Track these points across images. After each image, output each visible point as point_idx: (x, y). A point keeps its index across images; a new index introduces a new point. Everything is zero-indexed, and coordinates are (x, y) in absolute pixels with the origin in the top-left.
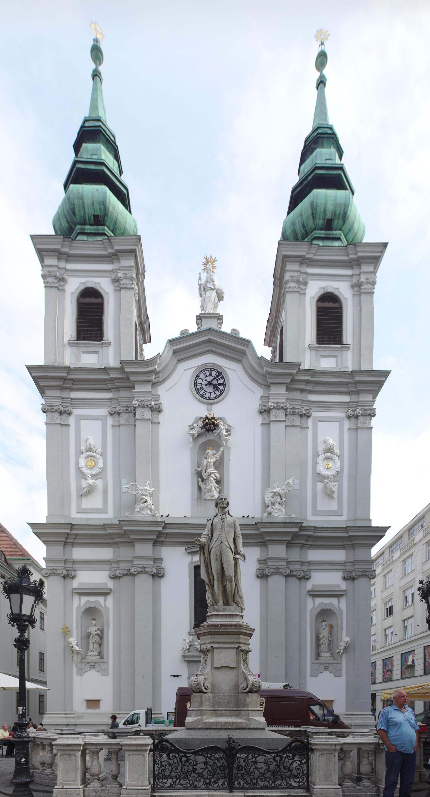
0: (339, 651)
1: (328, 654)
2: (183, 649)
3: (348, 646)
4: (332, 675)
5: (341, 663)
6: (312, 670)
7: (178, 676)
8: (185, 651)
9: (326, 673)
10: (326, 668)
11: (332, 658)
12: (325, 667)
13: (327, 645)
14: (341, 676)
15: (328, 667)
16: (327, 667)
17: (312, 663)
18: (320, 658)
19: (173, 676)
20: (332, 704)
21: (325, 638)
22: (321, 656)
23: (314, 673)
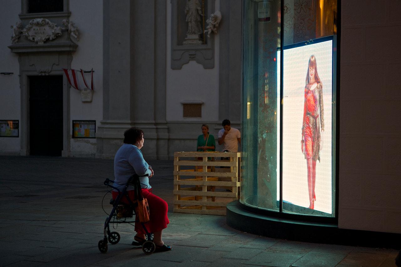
0: (207, 31)
1: (196, 37)
2: (12, 37)
3: (221, 23)
4: (201, 67)
5: (213, 49)
6: (173, 60)
7: (9, 74)
8: (14, 40)
9: (193, 63)
10: (192, 57)
11: (200, 42)
12: (191, 55)
13: (193, 23)
14: (212, 67)
15: (195, 55)
16: (193, 55)
17: (173, 50)
18: (184, 42)
19: (4, 73)
20: (200, 109)
21: (190, 13)
22: (186, 40)
23: (177, 66)
